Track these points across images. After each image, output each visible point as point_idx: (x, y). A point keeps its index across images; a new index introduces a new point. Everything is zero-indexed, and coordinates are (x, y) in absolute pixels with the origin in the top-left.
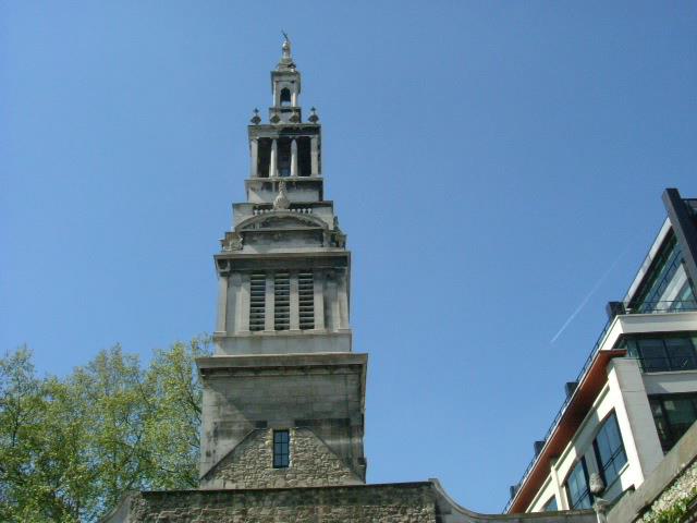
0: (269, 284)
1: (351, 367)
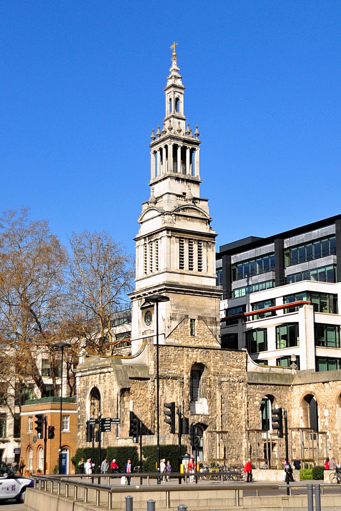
0: (186, 245)
1: (218, 295)
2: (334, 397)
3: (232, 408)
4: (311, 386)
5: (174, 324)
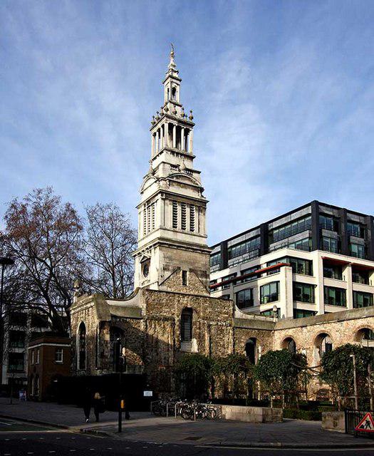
0: (179, 208)
3: (219, 348)
4: (291, 331)
5: (167, 274)
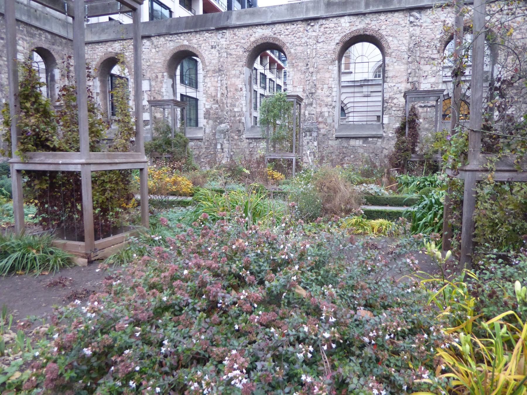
2: (160, 61)
